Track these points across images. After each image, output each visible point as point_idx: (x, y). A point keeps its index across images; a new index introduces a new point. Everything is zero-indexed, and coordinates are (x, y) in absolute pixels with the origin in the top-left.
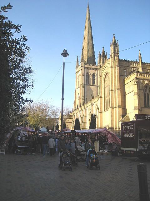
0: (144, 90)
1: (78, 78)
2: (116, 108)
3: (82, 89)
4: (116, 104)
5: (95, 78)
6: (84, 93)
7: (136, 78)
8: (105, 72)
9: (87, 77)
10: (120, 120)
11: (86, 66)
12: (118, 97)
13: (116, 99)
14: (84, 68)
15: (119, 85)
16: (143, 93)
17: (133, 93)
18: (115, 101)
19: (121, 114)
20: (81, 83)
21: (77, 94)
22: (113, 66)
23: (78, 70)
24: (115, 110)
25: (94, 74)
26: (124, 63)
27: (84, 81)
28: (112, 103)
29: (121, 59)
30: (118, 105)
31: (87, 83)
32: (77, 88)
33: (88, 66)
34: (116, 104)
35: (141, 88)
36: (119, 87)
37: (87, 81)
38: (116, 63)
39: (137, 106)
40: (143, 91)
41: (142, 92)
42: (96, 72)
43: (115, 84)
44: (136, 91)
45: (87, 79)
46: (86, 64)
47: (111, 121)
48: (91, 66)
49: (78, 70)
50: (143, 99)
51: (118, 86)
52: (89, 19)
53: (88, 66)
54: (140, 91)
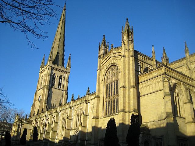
3: (46, 91)
4: (129, 107)
5: (61, 81)
6: (47, 96)
7: (165, 74)
13: (130, 100)
18: (129, 103)
21: (38, 97)
23: (43, 69)
28: (125, 105)
32: (38, 90)
34: (129, 107)
38: (131, 53)
39: (171, 111)
43: (129, 79)
48: (60, 68)
52: (64, 19)
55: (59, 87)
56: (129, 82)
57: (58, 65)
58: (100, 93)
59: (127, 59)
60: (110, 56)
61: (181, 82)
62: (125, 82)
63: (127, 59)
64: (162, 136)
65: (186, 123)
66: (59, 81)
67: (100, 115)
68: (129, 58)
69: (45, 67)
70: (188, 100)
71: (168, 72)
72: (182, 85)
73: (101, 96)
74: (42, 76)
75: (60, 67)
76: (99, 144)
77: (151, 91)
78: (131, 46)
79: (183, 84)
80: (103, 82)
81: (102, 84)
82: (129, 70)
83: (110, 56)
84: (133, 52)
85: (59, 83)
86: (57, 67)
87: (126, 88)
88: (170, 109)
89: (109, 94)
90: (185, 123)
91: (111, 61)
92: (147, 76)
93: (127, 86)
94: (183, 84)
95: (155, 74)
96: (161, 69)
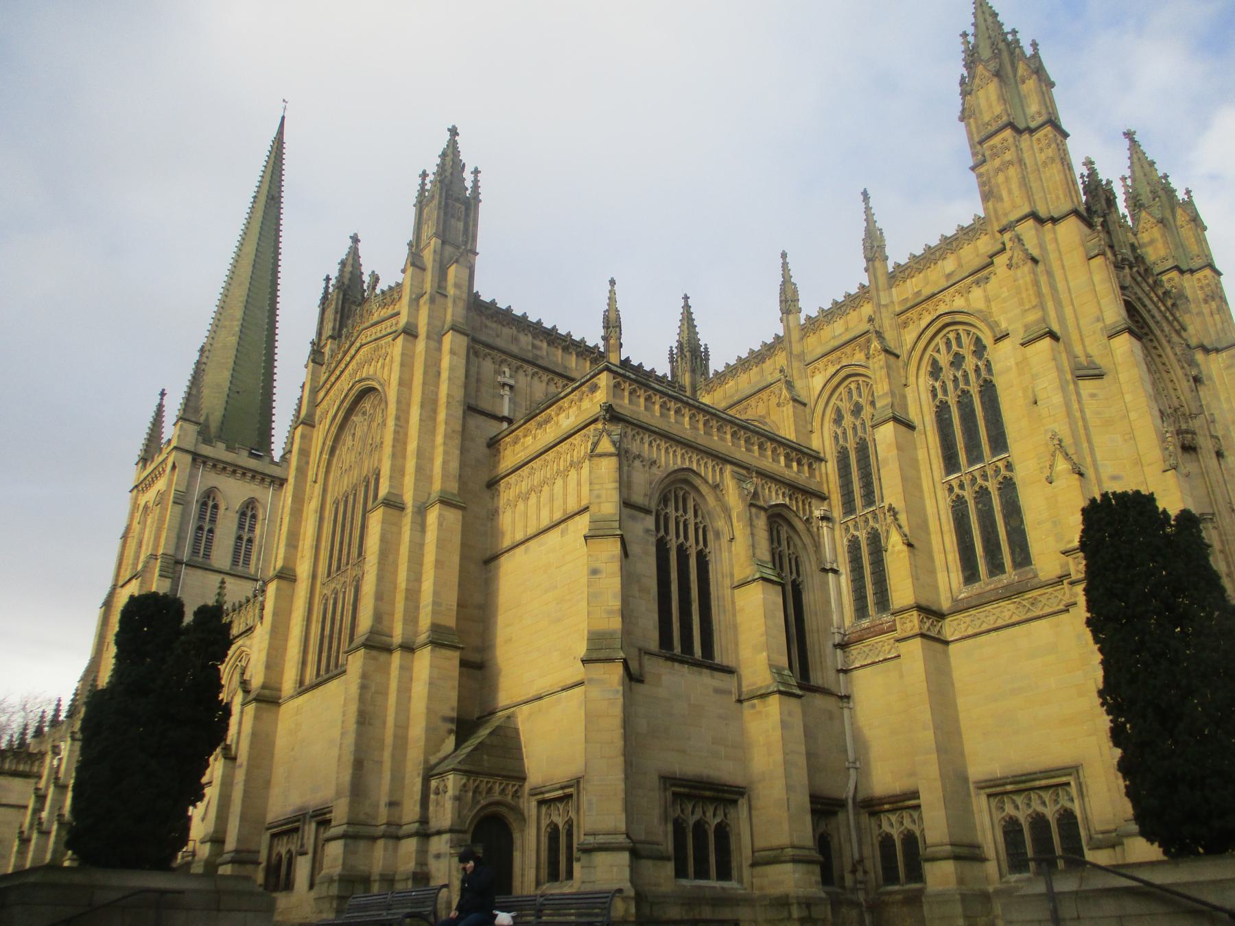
0: (662, 522)
1: (143, 523)
2: (409, 648)
4: (411, 617)
5: (252, 529)
7: (612, 415)
8: (344, 384)
9: (201, 517)
10: (441, 755)
11: (206, 450)
12: (438, 564)
14: (189, 458)
15: (454, 465)
16: (653, 540)
17: (582, 524)
18: (413, 595)
19: (454, 695)
20: (156, 546)
22: (422, 330)
23: (149, 469)
24: (406, 669)
25: (248, 512)
26: (507, 331)
27: (180, 538)
29: (486, 297)
30: (435, 628)
31: (195, 552)
32: (121, 583)
33: (218, 451)
34: (411, 617)
35: (638, 498)
36: (454, 487)
37: (197, 540)
40: (650, 522)
41: (647, 531)
42: (265, 495)
43: (424, 457)
44: (609, 506)
45: (200, 528)
46: (207, 441)
47: (358, 764)
48: (243, 459)
49: (149, 469)
50: (652, 584)
51: (445, 476)
53: (218, 451)
54: (633, 518)
55: (235, 562)
56: (422, 471)
57: (230, 448)
58: (299, 555)
59: (421, 345)
60: (358, 344)
61: (728, 468)
62: (398, 472)
63: (421, 345)
64: (577, 782)
65: (740, 701)
66: (241, 526)
67: (288, 683)
68: (436, 337)
69: (161, 458)
70: (761, 564)
71: (635, 406)
72: (730, 484)
73: (303, 570)
74: (146, 507)
75: (245, 453)
76: (263, 856)
77: (545, 522)
78: (452, 271)
79: (735, 476)
80: (318, 488)
81: (311, 507)
82: (430, 404)
83: (358, 344)
84: (461, 304)
85: (240, 538)
86: (229, 457)
87: (401, 508)
88: (610, 612)
89: (340, 560)
90: (734, 698)
91: (361, 365)
92: (529, 439)
93: (408, 498)
94: (733, 477)
95: (566, 419)
96: (594, 388)
